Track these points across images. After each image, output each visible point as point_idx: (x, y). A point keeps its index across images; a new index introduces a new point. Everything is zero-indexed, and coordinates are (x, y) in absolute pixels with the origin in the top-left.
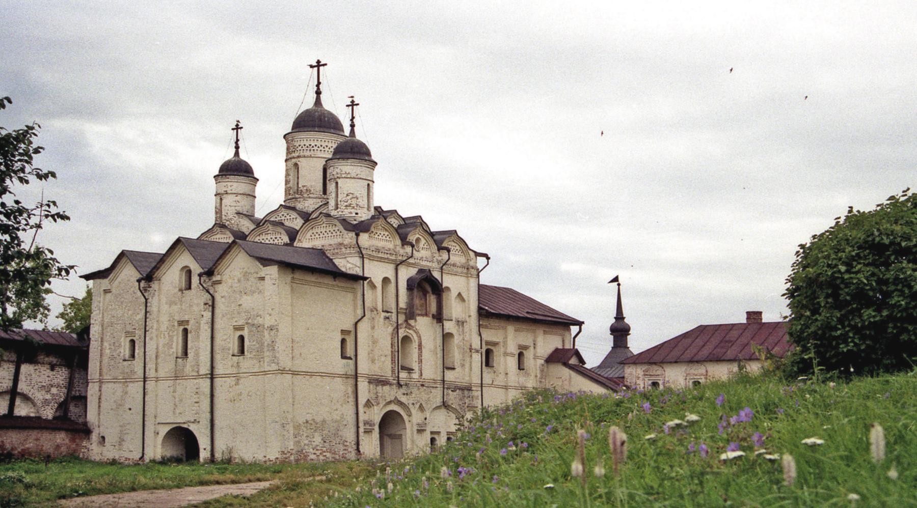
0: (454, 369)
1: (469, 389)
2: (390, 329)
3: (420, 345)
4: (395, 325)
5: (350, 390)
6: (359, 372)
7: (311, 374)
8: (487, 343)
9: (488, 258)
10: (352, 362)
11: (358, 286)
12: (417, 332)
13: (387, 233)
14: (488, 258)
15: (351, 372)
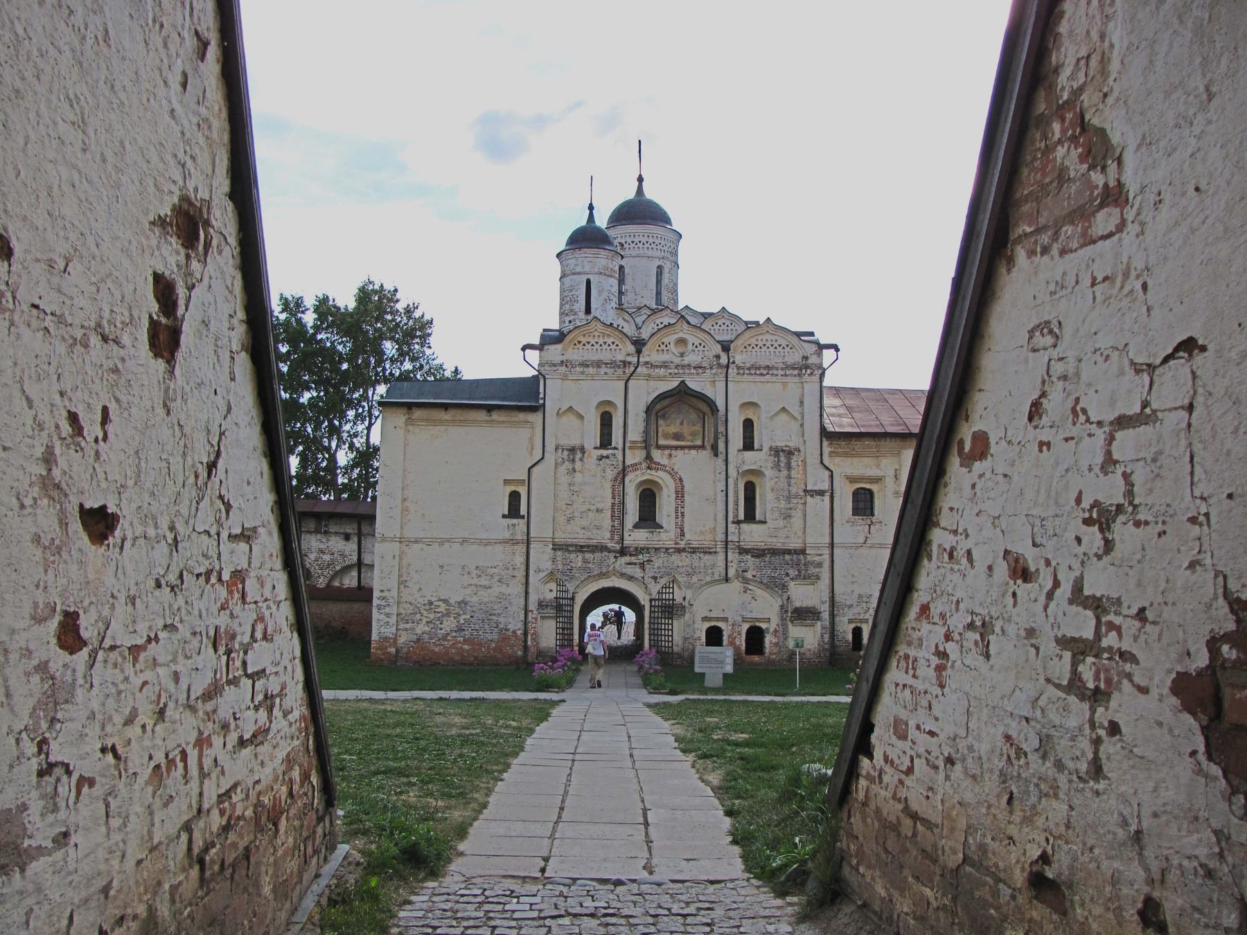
0: (765, 522)
1: (803, 552)
2: (610, 474)
3: (680, 494)
4: (621, 467)
5: (519, 559)
6: (532, 535)
7: (442, 542)
8: (852, 480)
9: (837, 350)
10: (522, 522)
11: (536, 418)
12: (672, 473)
13: (609, 341)
14: (837, 350)
15: (520, 536)
